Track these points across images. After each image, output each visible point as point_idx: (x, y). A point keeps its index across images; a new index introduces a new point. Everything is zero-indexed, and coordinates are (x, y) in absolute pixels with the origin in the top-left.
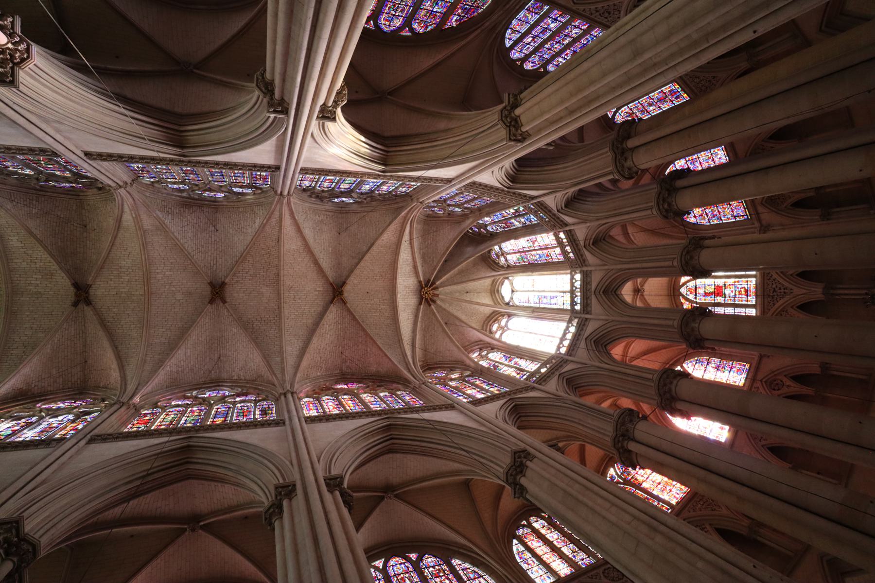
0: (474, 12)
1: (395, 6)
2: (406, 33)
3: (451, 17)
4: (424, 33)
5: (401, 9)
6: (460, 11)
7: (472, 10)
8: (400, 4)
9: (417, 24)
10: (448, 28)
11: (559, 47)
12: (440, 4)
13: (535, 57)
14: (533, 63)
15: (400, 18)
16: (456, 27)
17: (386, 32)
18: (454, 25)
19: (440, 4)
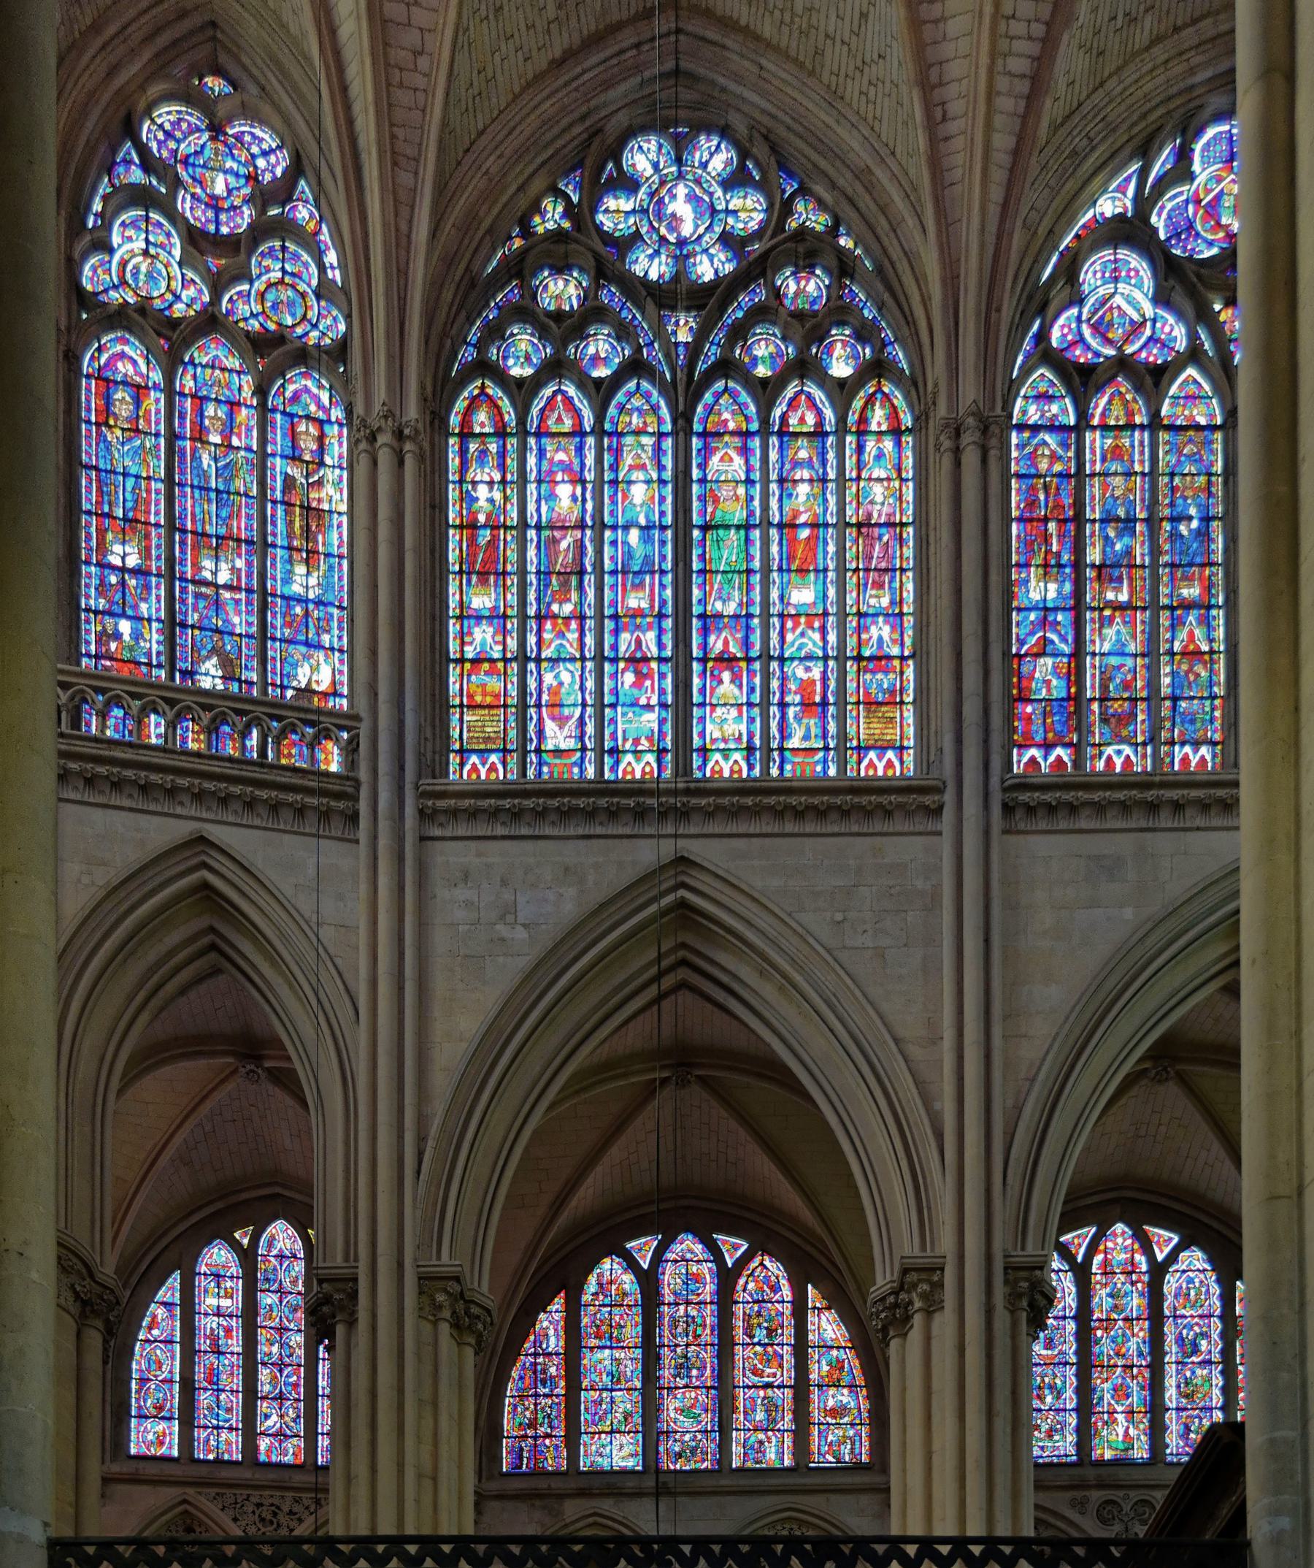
0: (521, 1378)
1: (696, 1336)
2: (643, 1248)
3: (562, 1343)
4: (597, 1261)
5: (679, 1330)
6: (553, 1371)
7: (527, 1381)
8: (687, 1345)
9: (627, 1287)
10: (550, 1302)
11: (265, 1349)
12: (604, 1376)
13: (294, 1282)
14: (281, 1257)
15: (672, 1299)
16: (538, 1314)
17: (686, 1231)
18: (542, 1316)
19: (604, 1376)
